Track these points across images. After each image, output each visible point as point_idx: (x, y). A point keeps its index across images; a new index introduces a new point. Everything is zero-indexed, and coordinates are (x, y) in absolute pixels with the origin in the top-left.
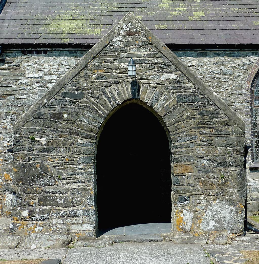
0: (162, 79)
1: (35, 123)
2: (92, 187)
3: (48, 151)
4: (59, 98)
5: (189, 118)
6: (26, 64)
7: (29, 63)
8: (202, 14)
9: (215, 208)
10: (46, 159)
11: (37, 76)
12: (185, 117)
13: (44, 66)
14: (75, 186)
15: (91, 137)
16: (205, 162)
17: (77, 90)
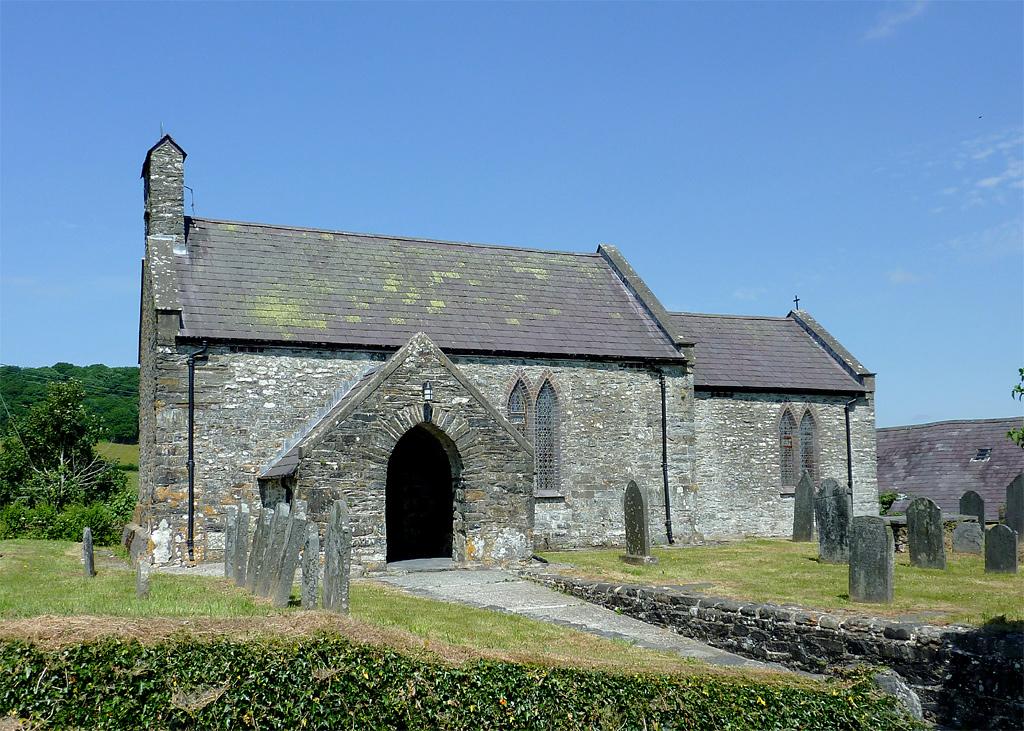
0: (454, 402)
1: (326, 447)
2: (383, 514)
3: (340, 476)
4: (351, 420)
5: (480, 443)
6: (235, 364)
7: (241, 364)
8: (441, 304)
9: (505, 536)
10: (338, 485)
11: (250, 380)
12: (476, 442)
13: (260, 368)
14: (366, 514)
15: (383, 462)
16: (496, 488)
17: (368, 412)
